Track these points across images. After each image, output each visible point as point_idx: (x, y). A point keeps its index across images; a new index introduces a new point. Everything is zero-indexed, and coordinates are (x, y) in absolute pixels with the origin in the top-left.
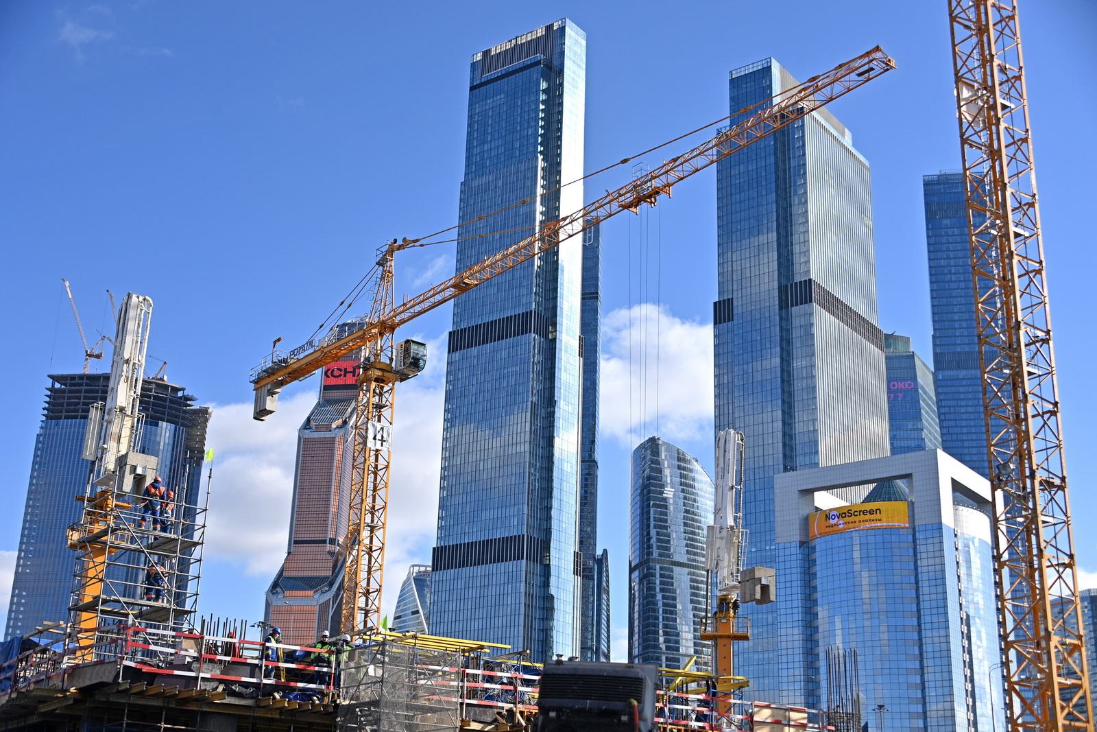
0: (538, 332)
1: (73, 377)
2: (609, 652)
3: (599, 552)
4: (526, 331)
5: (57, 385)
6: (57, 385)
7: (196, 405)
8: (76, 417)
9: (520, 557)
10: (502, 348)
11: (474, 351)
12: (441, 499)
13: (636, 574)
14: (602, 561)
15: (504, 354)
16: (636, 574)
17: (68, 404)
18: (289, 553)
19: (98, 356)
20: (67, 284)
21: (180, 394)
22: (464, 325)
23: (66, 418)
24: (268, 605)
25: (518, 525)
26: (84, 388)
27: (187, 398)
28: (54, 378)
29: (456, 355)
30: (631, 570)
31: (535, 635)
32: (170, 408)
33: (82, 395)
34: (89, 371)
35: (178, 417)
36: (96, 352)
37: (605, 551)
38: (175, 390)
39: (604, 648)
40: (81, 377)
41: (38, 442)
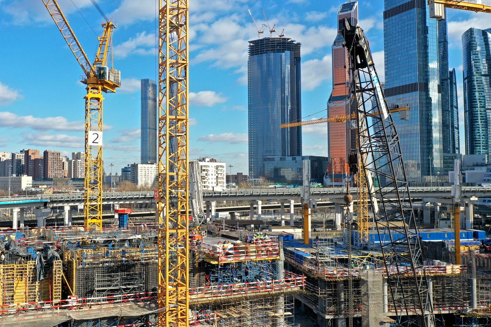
0: (418, 7)
1: (256, 41)
2: (457, 105)
3: (450, 69)
4: (413, 7)
5: (251, 44)
6: (251, 44)
7: (295, 43)
8: (258, 54)
9: (416, 90)
10: (404, 15)
11: (394, 17)
12: (386, 72)
13: (466, 81)
14: (453, 73)
15: (405, 17)
16: (466, 81)
17: (256, 50)
18: (333, 89)
19: (262, 33)
20: (249, 10)
21: (290, 40)
22: (389, 8)
23: (256, 54)
24: (328, 107)
25: (414, 78)
26: (260, 44)
27: (292, 41)
28: (250, 42)
29: (387, 20)
30: (464, 79)
31: (424, 116)
32: (288, 46)
33: (259, 46)
34: (261, 38)
35: (290, 48)
36: (261, 31)
37: (454, 69)
38: (288, 39)
39: (455, 104)
40: (258, 40)
41: (248, 63)
